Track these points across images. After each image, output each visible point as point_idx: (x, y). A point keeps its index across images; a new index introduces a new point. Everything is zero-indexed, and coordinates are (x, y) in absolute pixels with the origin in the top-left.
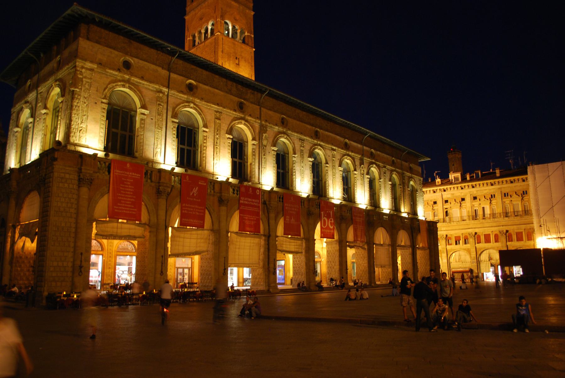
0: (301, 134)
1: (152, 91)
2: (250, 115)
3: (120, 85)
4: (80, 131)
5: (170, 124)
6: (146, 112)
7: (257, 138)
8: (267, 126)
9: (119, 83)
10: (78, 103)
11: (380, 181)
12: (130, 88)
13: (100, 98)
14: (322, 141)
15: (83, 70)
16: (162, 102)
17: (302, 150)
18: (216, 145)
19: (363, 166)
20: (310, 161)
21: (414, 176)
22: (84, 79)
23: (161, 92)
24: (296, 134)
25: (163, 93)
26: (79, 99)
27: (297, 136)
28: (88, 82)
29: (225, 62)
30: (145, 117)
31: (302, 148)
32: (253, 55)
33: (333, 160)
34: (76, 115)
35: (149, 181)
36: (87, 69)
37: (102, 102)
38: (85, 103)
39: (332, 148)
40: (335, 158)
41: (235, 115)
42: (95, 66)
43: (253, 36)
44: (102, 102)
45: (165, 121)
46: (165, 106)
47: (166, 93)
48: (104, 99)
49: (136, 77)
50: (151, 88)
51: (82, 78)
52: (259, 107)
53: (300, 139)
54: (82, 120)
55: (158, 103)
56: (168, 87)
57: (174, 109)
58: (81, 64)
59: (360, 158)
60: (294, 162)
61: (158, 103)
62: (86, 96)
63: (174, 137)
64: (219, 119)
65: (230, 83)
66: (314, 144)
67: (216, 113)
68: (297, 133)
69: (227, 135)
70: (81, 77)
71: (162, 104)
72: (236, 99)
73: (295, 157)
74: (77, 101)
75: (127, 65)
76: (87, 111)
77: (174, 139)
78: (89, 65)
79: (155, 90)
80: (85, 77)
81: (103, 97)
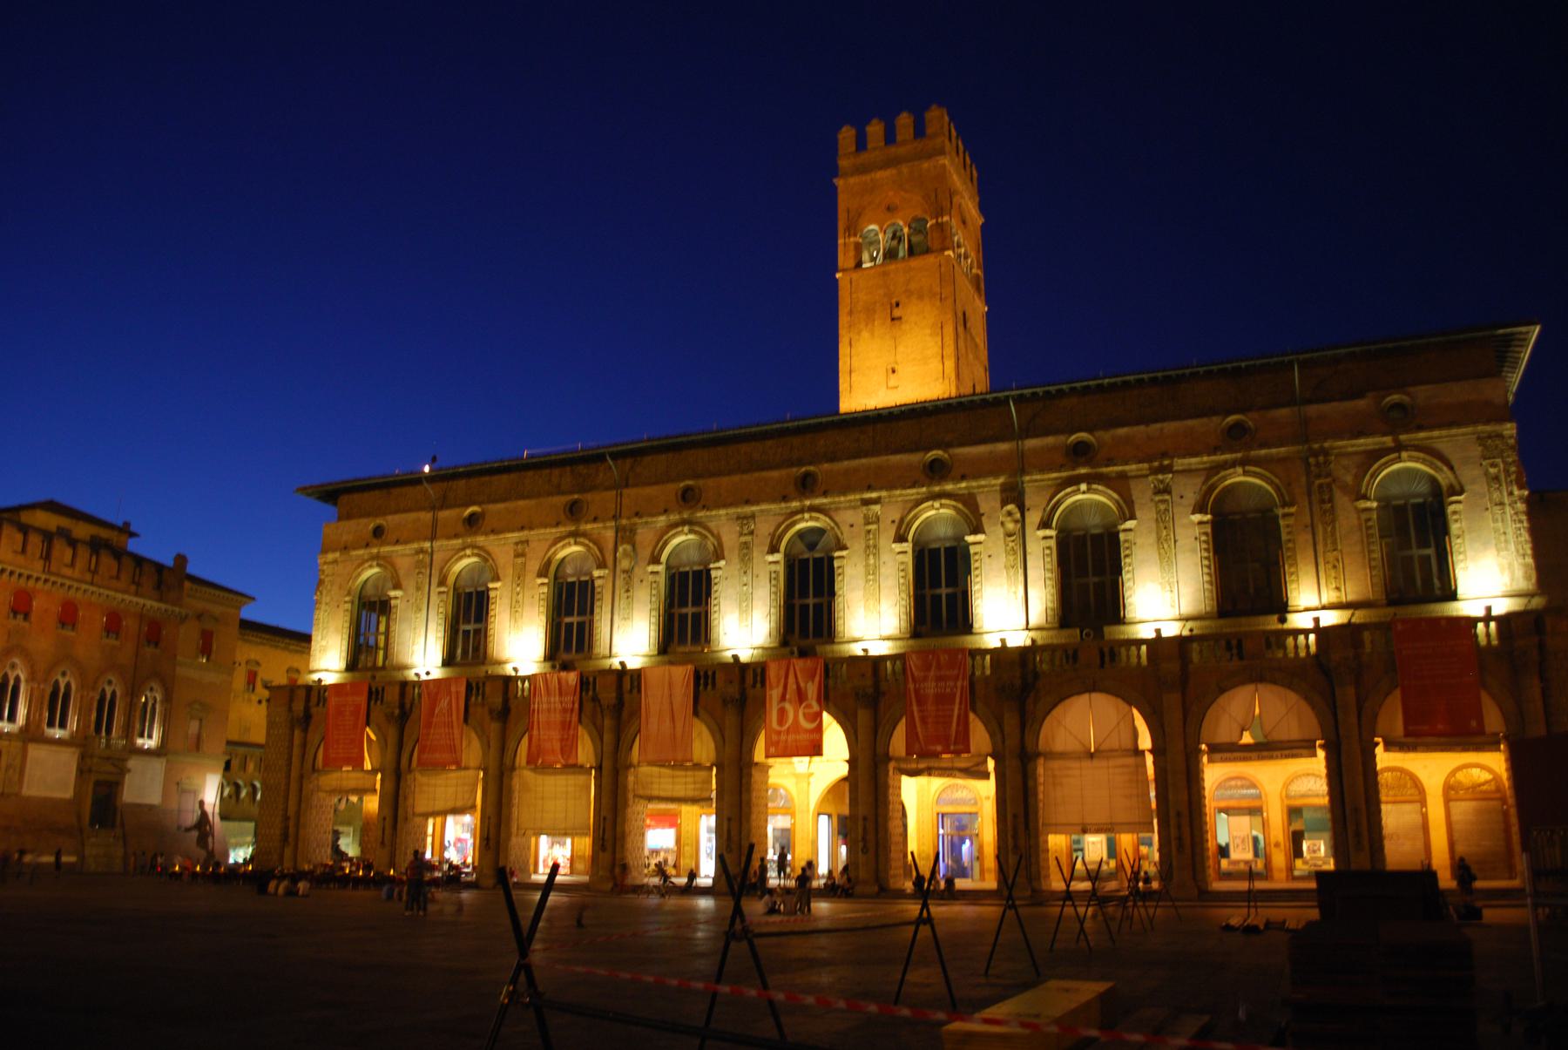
5: (434, 598)
7: (610, 562)
8: (635, 524)
15: (325, 567)
17: (745, 543)
19: (1011, 507)
21: (1422, 435)
23: (422, 551)
24: (722, 512)
29: (859, 333)
31: (743, 539)
33: (869, 532)
42: (337, 555)
45: (426, 596)
53: (738, 518)
58: (322, 561)
59: (1002, 485)
64: (522, 555)
68: (725, 506)
75: (378, 532)
76: (328, 622)
80: (327, 576)
81: (346, 593)
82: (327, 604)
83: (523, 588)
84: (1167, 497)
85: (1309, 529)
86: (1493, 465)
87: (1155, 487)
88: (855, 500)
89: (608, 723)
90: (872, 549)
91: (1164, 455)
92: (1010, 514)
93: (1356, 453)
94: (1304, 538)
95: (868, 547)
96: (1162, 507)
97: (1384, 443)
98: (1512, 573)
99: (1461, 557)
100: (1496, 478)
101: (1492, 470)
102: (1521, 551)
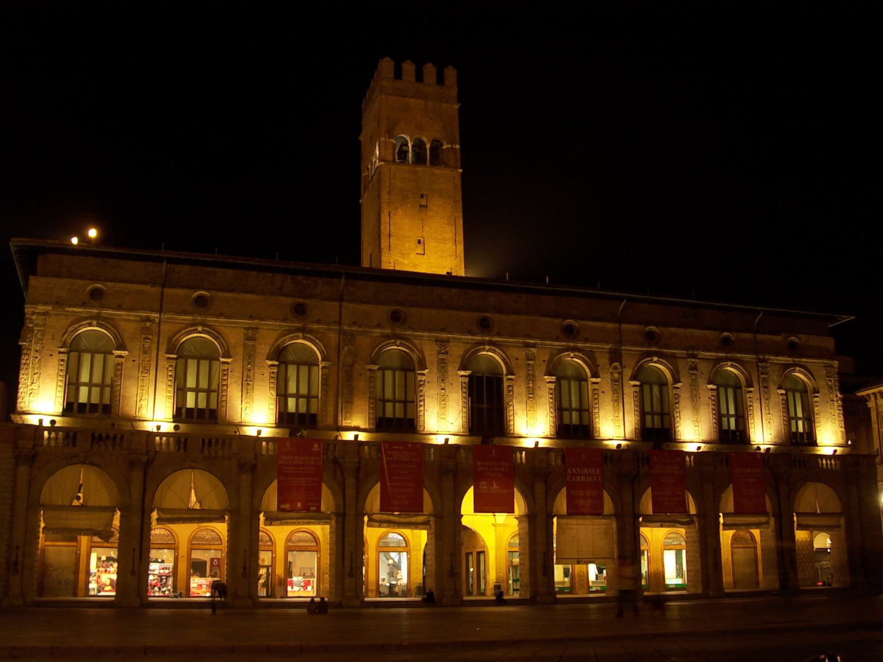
0: (443, 330)
1: (133, 321)
2: (319, 322)
3: (86, 324)
4: (30, 394)
6: (124, 353)
9: (85, 322)
10: (27, 359)
11: (678, 388)
12: (99, 325)
13: (58, 347)
14: (499, 334)
15: (34, 317)
16: (150, 334)
17: (442, 359)
18: (246, 381)
19: (616, 364)
20: (462, 376)
21: (804, 360)
22: (35, 328)
23: (148, 319)
24: (425, 334)
25: (152, 321)
26: (29, 354)
27: (429, 336)
28: (41, 330)
29: (396, 209)
30: (123, 360)
32: (458, 181)
33: (529, 365)
34: (24, 376)
35: (118, 448)
36: (39, 314)
37: (60, 353)
38: (36, 358)
39: (524, 343)
40: (533, 360)
41: (286, 326)
43: (458, 147)
44: (60, 353)
46: (156, 339)
47: (157, 320)
48: (61, 347)
49: (110, 308)
50: (132, 318)
51: (33, 327)
52: (338, 303)
53: (437, 340)
54: (33, 380)
55: (144, 336)
56: (160, 311)
57: (170, 339)
58: (31, 310)
59: (610, 349)
60: (422, 383)
61: (144, 336)
62: (38, 349)
63: (170, 380)
64: (254, 339)
65: (278, 277)
66: (476, 343)
67: (246, 332)
68: (430, 331)
69: (267, 361)
70: (32, 325)
71: (150, 337)
72: (289, 301)
73: (424, 374)
74: (26, 358)
75: (96, 295)
76: (39, 368)
77: (169, 383)
78: (41, 308)
79: (139, 319)
80: (37, 325)
81: (61, 344)
82: (37, 351)
83: (254, 366)
84: (695, 372)
85: (759, 401)
86: (830, 381)
87: (690, 366)
88: (520, 343)
89: (350, 481)
90: (531, 378)
91: (693, 348)
92: (616, 368)
93: (777, 364)
94: (756, 405)
95: (528, 375)
96: (694, 377)
97: (788, 361)
98: (837, 435)
99: (819, 424)
100: (831, 387)
101: (830, 383)
102: (841, 425)
